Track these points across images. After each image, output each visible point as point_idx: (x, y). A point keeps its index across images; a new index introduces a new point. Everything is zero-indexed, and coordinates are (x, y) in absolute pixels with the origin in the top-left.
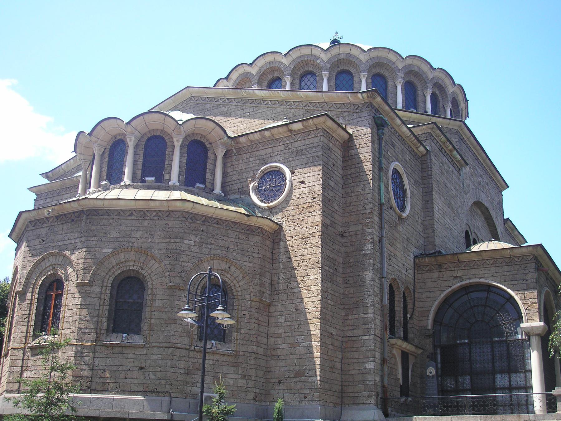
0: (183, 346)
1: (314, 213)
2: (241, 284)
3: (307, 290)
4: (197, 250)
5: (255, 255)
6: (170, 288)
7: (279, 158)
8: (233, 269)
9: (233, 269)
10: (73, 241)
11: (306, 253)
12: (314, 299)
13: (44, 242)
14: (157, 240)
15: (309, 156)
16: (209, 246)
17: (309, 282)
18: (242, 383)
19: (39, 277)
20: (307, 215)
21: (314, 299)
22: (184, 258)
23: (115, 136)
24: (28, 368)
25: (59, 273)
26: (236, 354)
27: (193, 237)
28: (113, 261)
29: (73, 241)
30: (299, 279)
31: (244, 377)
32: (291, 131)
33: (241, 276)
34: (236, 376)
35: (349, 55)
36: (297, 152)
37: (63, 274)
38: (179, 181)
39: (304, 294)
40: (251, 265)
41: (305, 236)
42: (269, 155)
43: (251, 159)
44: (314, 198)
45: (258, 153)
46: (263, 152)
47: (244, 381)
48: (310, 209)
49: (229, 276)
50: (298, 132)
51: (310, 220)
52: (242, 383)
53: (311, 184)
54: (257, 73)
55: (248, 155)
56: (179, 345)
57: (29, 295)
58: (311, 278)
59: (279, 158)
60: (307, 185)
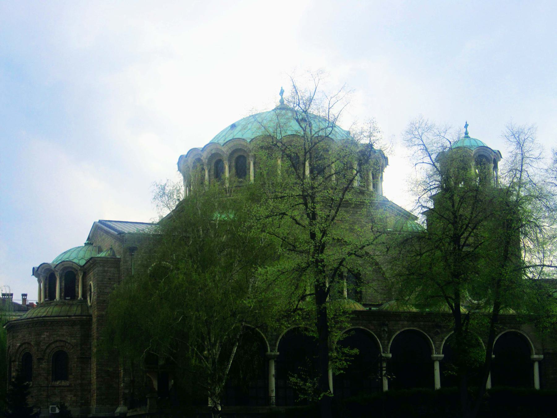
0: (45, 385)
2: (71, 351)
4: (48, 339)
5: (77, 335)
6: (38, 359)
8: (67, 344)
9: (67, 344)
14: (33, 337)
16: (54, 336)
18: (74, 399)
22: (42, 344)
26: (70, 386)
27: (46, 333)
28: (21, 349)
31: (75, 396)
33: (71, 347)
34: (72, 396)
38: (60, 296)
40: (75, 341)
47: (75, 398)
49: (65, 349)
52: (74, 399)
56: (43, 385)
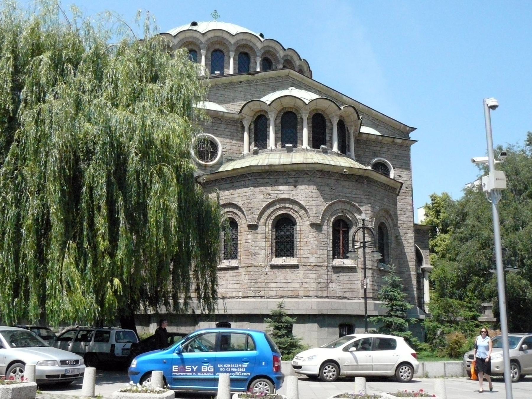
1: (407, 197)
3: (407, 242)
7: (384, 155)
10: (359, 196)
11: (405, 220)
12: (411, 248)
13: (334, 191)
15: (402, 161)
17: (408, 238)
19: (332, 216)
20: (404, 197)
21: (411, 248)
23: (317, 110)
24: (332, 281)
25: (348, 216)
29: (359, 196)
30: (401, 235)
32: (393, 141)
35: (292, 57)
36: (396, 156)
37: (351, 217)
39: (405, 244)
41: (404, 210)
42: (378, 152)
43: (367, 150)
44: (407, 188)
45: (372, 148)
46: (375, 148)
48: (405, 194)
50: (396, 144)
51: (406, 201)
53: (405, 179)
54: (235, 43)
55: (364, 147)
57: (324, 227)
58: (409, 235)
59: (385, 156)
60: (403, 179)
